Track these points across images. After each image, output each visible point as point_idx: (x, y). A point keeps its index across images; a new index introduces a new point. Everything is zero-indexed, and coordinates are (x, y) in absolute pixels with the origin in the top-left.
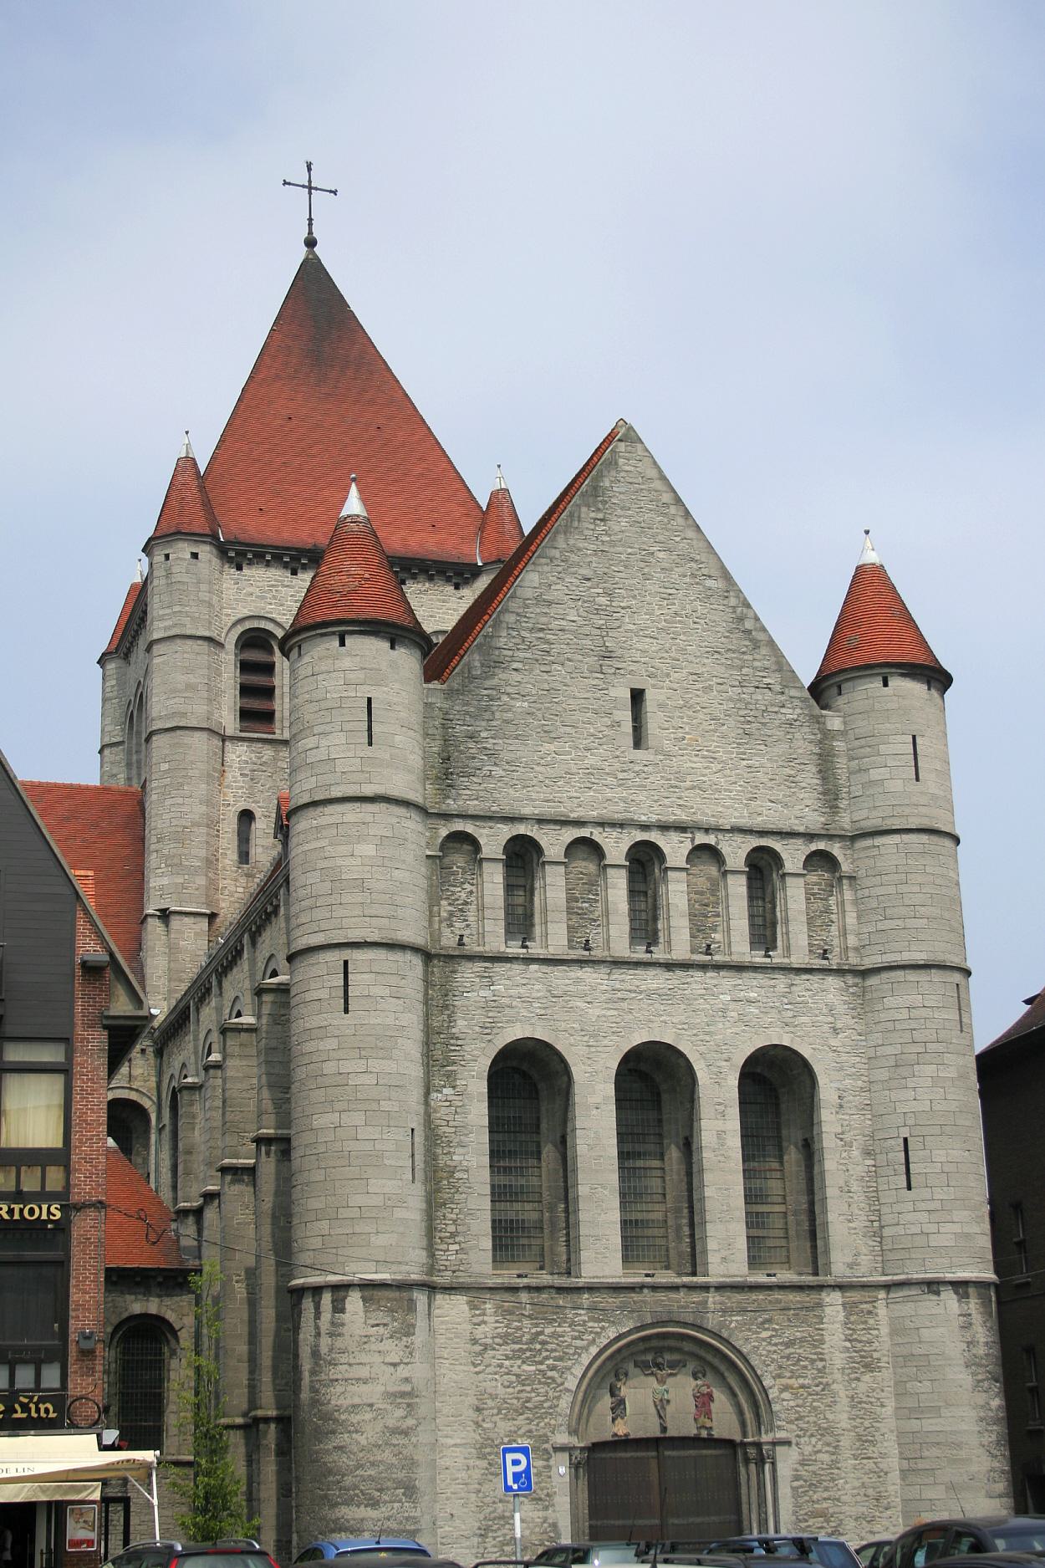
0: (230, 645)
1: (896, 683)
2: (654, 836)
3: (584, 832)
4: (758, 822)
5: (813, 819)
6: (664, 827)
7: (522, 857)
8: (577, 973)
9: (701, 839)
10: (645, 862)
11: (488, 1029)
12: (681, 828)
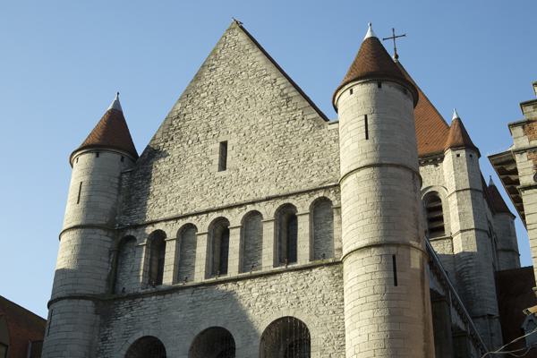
2: (225, 214)
3: (189, 220)
4: (282, 192)
5: (316, 182)
6: (230, 207)
7: (159, 240)
9: (250, 208)
10: (220, 231)
11: (126, 335)
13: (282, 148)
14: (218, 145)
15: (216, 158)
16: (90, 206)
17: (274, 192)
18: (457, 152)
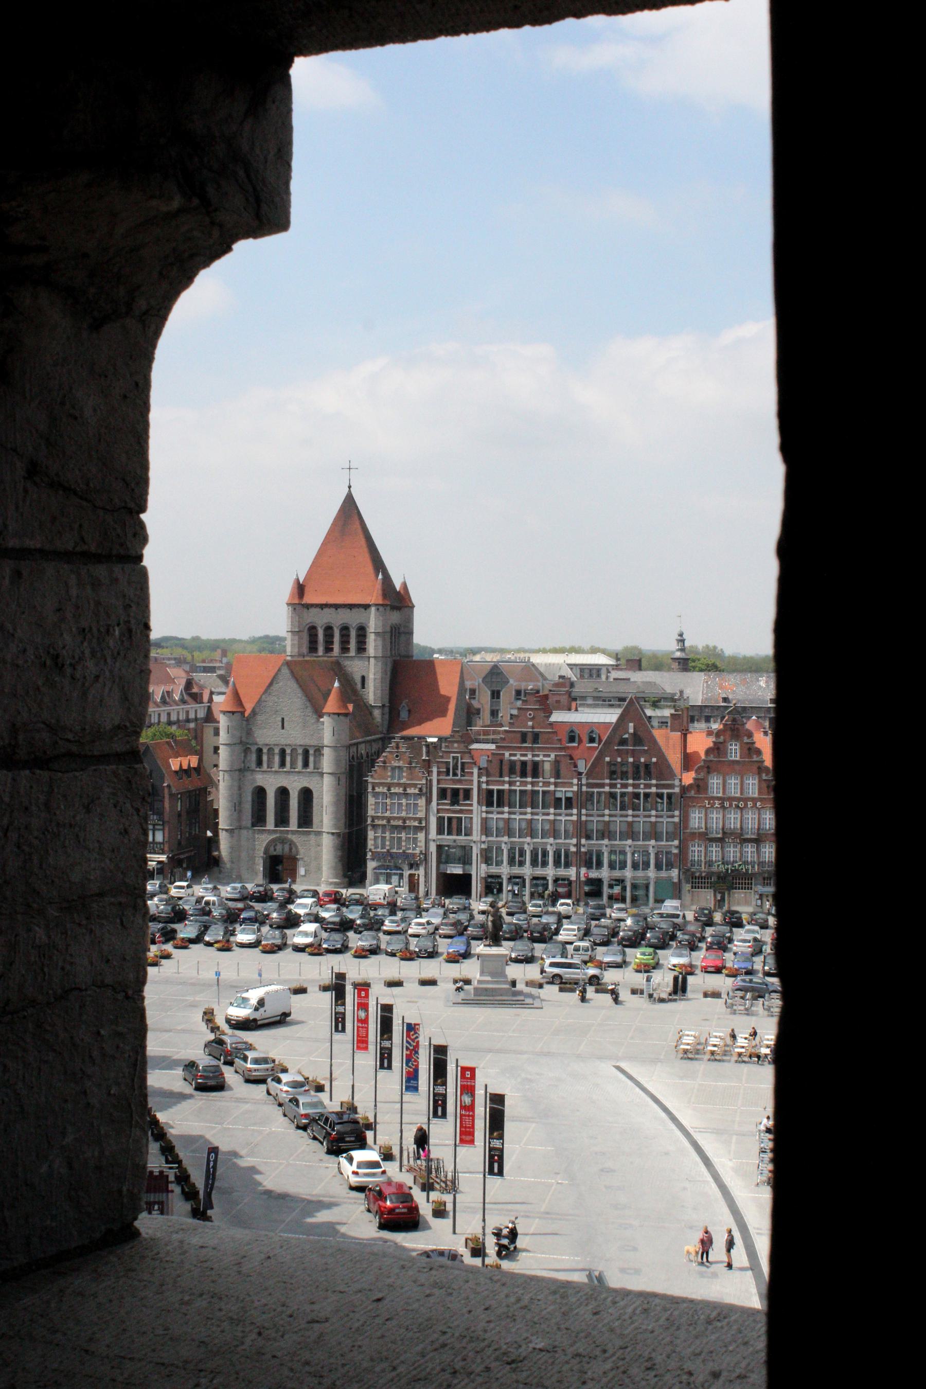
0: (306, 630)
7: (260, 751)
10: (283, 753)
14: (280, 719)
15: (280, 724)
16: (233, 736)
17: (301, 743)
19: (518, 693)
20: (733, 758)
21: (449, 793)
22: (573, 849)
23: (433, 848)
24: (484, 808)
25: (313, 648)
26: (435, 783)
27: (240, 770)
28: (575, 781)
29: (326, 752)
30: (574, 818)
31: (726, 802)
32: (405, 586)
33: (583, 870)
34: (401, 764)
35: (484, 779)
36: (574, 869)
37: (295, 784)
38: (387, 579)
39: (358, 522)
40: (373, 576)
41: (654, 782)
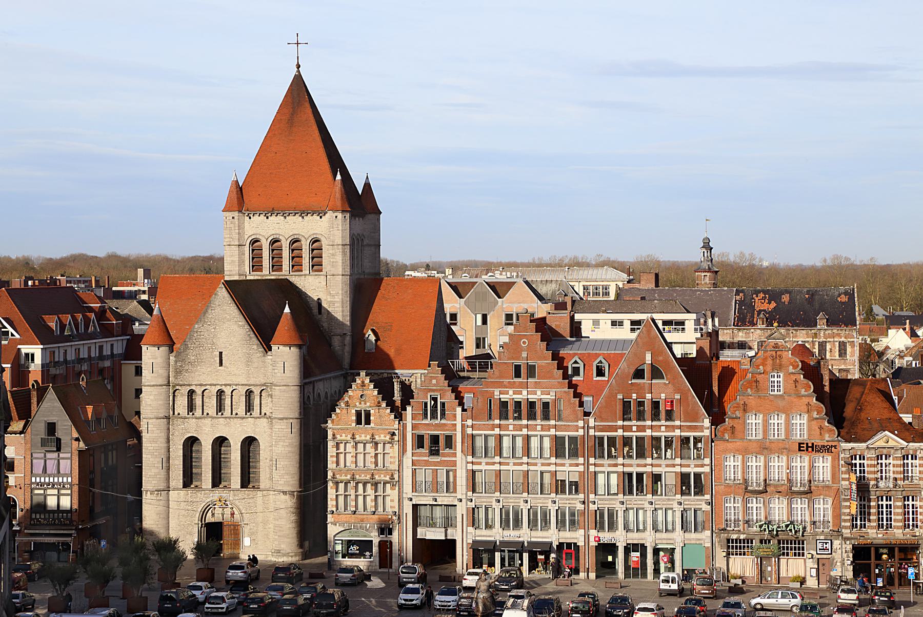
1: (281, 347)
2: (223, 388)
5: (263, 381)
6: (226, 385)
7: (191, 393)
8: (203, 420)
10: (220, 393)
11: (183, 434)
12: (230, 385)
13: (249, 362)
18: (336, 214)
19: (509, 317)
20: (776, 392)
21: (427, 442)
22: (580, 507)
23: (408, 510)
24: (470, 458)
25: (256, 265)
26: (409, 428)
27: (168, 418)
28: (581, 423)
29: (276, 391)
30: (581, 468)
31: (765, 448)
32: (367, 186)
33: (593, 533)
34: (368, 404)
35: (469, 422)
36: (582, 532)
37: (235, 434)
38: (347, 179)
39: (309, 110)
40: (329, 175)
41: (677, 423)
